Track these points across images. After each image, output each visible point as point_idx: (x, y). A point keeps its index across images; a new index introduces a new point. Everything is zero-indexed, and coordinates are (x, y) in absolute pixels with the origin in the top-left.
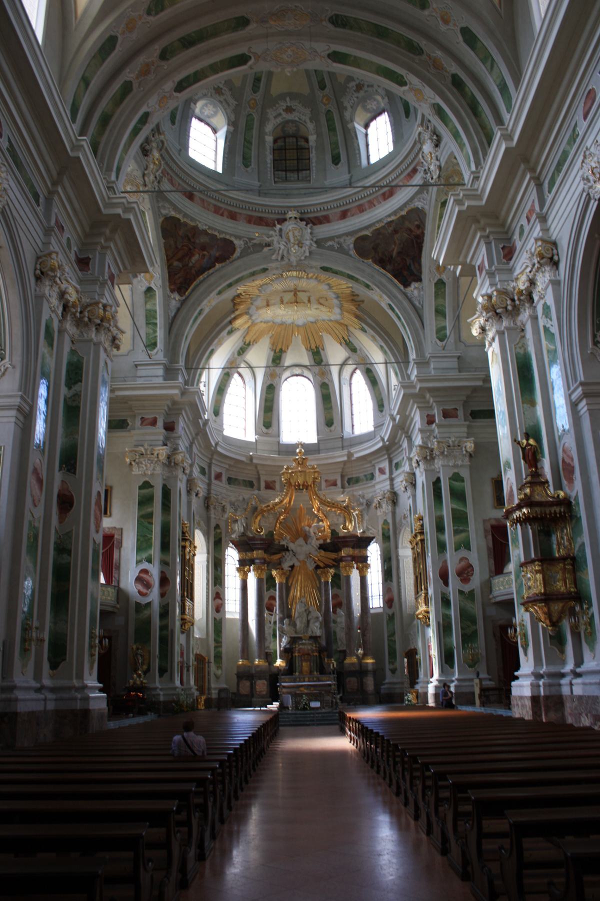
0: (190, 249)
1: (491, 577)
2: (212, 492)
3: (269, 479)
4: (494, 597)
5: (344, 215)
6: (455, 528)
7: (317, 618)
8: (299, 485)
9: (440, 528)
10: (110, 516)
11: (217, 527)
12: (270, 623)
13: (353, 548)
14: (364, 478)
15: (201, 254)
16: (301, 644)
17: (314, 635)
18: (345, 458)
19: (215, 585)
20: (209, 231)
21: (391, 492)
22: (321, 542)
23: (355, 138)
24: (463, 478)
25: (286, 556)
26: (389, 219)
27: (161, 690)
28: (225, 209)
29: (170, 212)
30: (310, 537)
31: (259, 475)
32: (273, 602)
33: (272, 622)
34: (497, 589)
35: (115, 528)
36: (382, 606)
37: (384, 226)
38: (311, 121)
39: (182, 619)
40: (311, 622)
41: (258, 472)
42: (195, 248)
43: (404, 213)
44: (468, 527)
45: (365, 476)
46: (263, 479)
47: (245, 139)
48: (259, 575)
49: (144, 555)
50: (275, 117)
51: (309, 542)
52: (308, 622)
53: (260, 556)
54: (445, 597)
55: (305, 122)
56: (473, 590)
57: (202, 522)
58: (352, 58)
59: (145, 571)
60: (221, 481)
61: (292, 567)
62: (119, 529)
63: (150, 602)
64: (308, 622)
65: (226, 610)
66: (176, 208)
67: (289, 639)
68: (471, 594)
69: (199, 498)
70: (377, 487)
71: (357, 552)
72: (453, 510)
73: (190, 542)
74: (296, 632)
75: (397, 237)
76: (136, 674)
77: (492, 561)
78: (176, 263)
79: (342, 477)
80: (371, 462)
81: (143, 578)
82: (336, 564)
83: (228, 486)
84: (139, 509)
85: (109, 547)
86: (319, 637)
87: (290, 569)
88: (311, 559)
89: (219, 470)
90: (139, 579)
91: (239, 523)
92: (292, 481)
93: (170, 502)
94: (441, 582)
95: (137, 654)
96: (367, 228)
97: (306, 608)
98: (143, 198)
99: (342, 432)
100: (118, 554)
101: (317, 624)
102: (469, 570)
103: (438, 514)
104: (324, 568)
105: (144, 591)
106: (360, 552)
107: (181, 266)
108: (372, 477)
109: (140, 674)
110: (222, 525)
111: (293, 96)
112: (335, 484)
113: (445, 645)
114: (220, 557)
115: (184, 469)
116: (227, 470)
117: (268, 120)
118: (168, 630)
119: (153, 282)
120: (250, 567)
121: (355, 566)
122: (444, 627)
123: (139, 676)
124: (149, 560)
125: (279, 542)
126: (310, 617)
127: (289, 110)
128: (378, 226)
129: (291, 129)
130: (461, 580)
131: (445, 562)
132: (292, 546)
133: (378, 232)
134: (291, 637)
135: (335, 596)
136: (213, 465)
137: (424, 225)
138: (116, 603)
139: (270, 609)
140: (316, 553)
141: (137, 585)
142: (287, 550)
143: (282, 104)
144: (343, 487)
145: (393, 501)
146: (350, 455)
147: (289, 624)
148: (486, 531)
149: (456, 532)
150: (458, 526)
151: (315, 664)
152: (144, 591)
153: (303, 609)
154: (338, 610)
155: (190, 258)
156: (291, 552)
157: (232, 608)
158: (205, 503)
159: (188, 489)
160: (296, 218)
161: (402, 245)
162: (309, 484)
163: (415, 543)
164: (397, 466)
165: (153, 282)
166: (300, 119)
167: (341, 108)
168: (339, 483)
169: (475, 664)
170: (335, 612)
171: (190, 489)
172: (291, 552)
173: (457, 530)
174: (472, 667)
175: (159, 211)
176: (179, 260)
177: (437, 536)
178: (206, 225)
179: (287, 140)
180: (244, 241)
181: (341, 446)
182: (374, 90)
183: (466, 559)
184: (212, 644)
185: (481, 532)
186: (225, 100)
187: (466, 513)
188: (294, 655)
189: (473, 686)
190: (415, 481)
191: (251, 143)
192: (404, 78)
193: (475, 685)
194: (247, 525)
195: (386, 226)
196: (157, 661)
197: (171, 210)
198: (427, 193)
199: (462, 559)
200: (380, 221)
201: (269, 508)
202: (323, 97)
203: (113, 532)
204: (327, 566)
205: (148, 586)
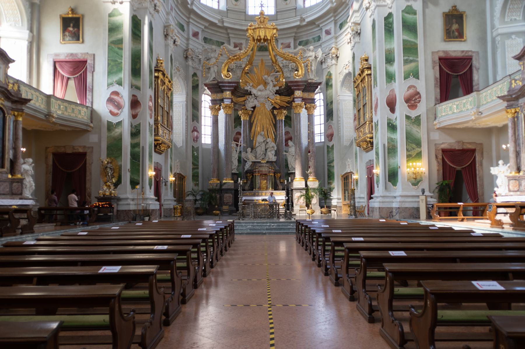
1: (436, 105)
2: (191, 47)
3: (238, 41)
4: (440, 123)
6: (406, 58)
7: (273, 147)
8: (261, 39)
9: (389, 60)
10: (83, 42)
11: (195, 75)
12: (236, 151)
13: (303, 92)
14: (313, 41)
16: (260, 166)
17: (270, 160)
18: (298, 23)
19: (193, 121)
21: (335, 48)
22: (277, 88)
24: (416, 11)
25: (249, 99)
27: (133, 200)
30: (268, 83)
31: (229, 38)
32: (239, 136)
33: (238, 152)
34: (440, 116)
35: (88, 53)
36: (323, 140)
39: (155, 140)
40: (268, 150)
41: (228, 34)
44: (418, 58)
45: (314, 38)
46: (232, 41)
48: (227, 112)
49: (115, 78)
51: (267, 87)
52: (266, 150)
53: (228, 96)
54: (390, 123)
56: (420, 116)
57: (181, 69)
59: (116, 93)
60: (198, 39)
61: (254, 108)
62: (91, 54)
63: (121, 121)
64: (266, 150)
65: (203, 142)
67: (251, 163)
68: (417, 120)
69: (176, 45)
70: (323, 46)
71: (306, 95)
72: (404, 41)
73: (164, 75)
74: (256, 157)
76: (106, 185)
77: (438, 90)
79: (295, 40)
80: (318, 26)
81: (113, 99)
82: (289, 105)
83: (203, 43)
84: (109, 35)
85: (83, 71)
86: (275, 162)
87: (252, 109)
88: (270, 101)
89: (196, 30)
90: (110, 100)
91: (212, 69)
92: (254, 36)
93: (141, 32)
94: (389, 109)
95: (107, 167)
97: (264, 139)
99: (296, 4)
100: (91, 77)
101: (273, 152)
102: (417, 97)
103: (388, 47)
104: (279, 109)
105: (115, 111)
106: (309, 95)
108: (319, 38)
109: (109, 186)
110: (199, 74)
112: (289, 46)
113: (389, 165)
114: (197, 99)
115: (155, 6)
116: (203, 31)
118: (140, 148)
120: (220, 106)
121: (304, 107)
122: (388, 149)
123: (109, 187)
124: (120, 83)
125: (244, 88)
126: (267, 146)
130: (408, 106)
131: (393, 91)
132: (254, 91)
134: (252, 162)
135: (287, 133)
136: (190, 24)
138: (90, 122)
139: (236, 140)
140: (273, 97)
141: (109, 105)
142: (250, 94)
144: (295, 48)
145: (337, 55)
146: (302, 20)
147: (251, 152)
148: (434, 62)
149: (406, 62)
150: (408, 57)
151: (271, 183)
152: (115, 111)
153: (262, 141)
154: (289, 141)
156: (253, 96)
157: (206, 139)
158: (184, 55)
159: (165, 33)
162: (269, 38)
163: (359, 81)
164: (341, 26)
168: (292, 45)
169: (418, 182)
170: (287, 145)
171: (168, 35)
172: (253, 96)
173: (407, 60)
174: (415, 186)
177: (386, 67)
181: (294, 16)
183: (414, 87)
184: (190, 166)
185: (430, 63)
187: (416, 45)
188: (254, 175)
189: (419, 202)
190: (360, 30)
193: (421, 202)
194: (217, 72)
196: (128, 175)
199: (410, 87)
201: (235, 57)
203: (86, 57)
204: (281, 108)
205: (119, 106)
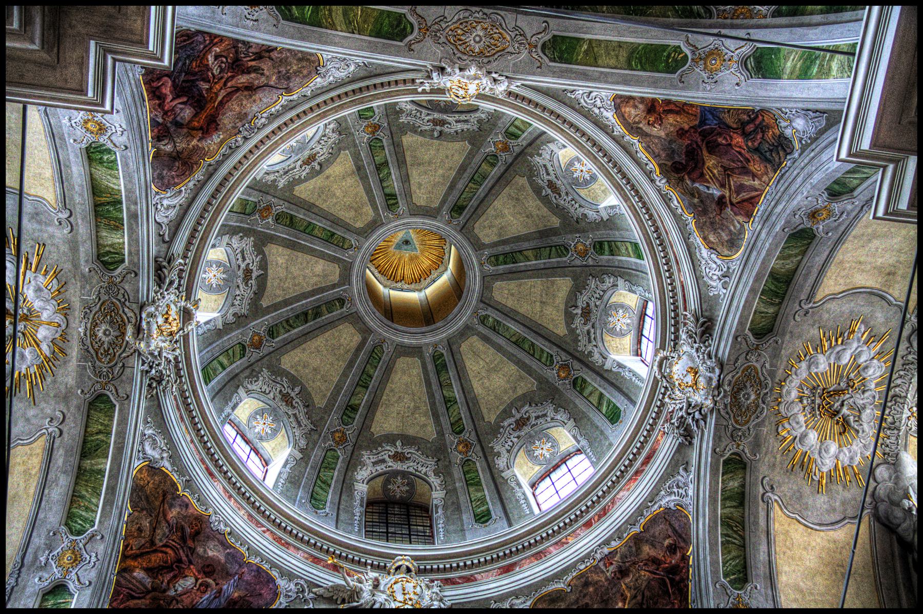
0: (180, 561)
5: (508, 569)
15: (200, 581)
20: (231, 540)
23: (517, 488)
26: (606, 550)
28: (268, 530)
29: (162, 458)
37: (596, 567)
38: (436, 473)
42: (190, 562)
43: (637, 529)
47: (318, 476)
50: (374, 464)
55: (425, 474)
58: (585, 47)
66: (175, 457)
75: (628, 580)
78: (139, 574)
96: (557, 576)
98: (124, 365)
107: (149, 586)
111: (408, 440)
117: (363, 465)
119: (74, 572)
127: (398, 457)
128: (582, 567)
129: (398, 489)
133: (584, 581)
137: (687, 542)
143: (388, 448)
155: (175, 577)
160: (409, 570)
161: (639, 598)
165: (74, 572)
166: (416, 471)
167: (488, 456)
175: (142, 443)
176: (147, 570)
178: (226, 525)
179: (390, 510)
180: (297, 584)
182: (549, 419)
186: (295, 415)
191: (329, 486)
192: (681, 52)
195: (601, 564)
197: (165, 455)
198: (686, 470)
200: (588, 556)
202: (459, 443)
